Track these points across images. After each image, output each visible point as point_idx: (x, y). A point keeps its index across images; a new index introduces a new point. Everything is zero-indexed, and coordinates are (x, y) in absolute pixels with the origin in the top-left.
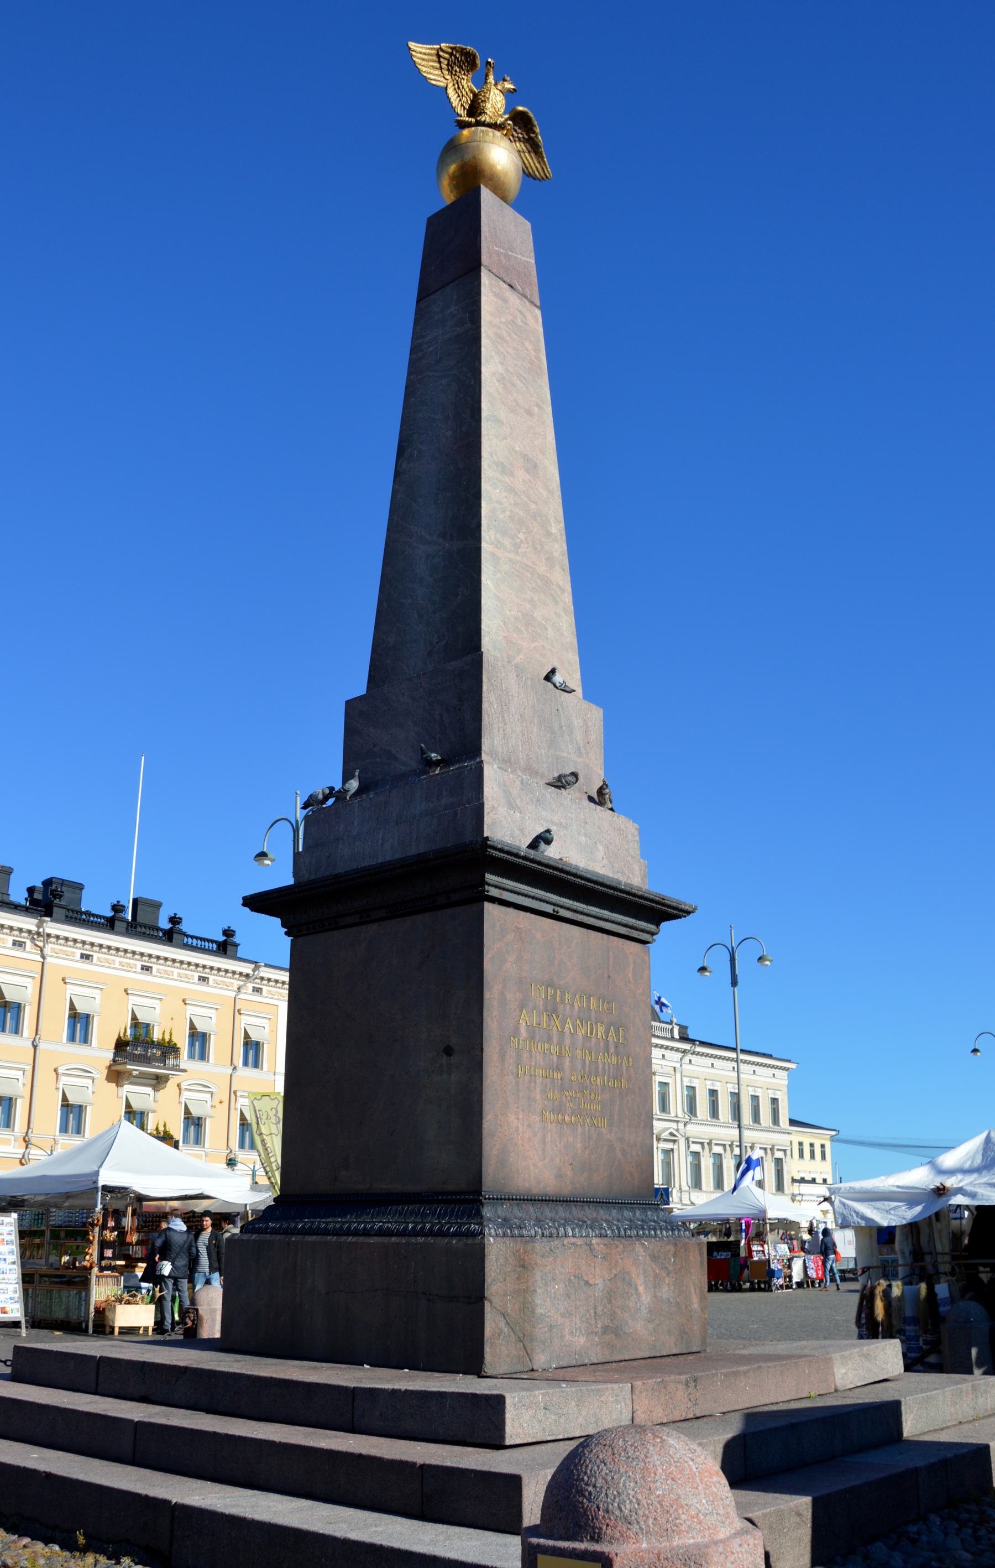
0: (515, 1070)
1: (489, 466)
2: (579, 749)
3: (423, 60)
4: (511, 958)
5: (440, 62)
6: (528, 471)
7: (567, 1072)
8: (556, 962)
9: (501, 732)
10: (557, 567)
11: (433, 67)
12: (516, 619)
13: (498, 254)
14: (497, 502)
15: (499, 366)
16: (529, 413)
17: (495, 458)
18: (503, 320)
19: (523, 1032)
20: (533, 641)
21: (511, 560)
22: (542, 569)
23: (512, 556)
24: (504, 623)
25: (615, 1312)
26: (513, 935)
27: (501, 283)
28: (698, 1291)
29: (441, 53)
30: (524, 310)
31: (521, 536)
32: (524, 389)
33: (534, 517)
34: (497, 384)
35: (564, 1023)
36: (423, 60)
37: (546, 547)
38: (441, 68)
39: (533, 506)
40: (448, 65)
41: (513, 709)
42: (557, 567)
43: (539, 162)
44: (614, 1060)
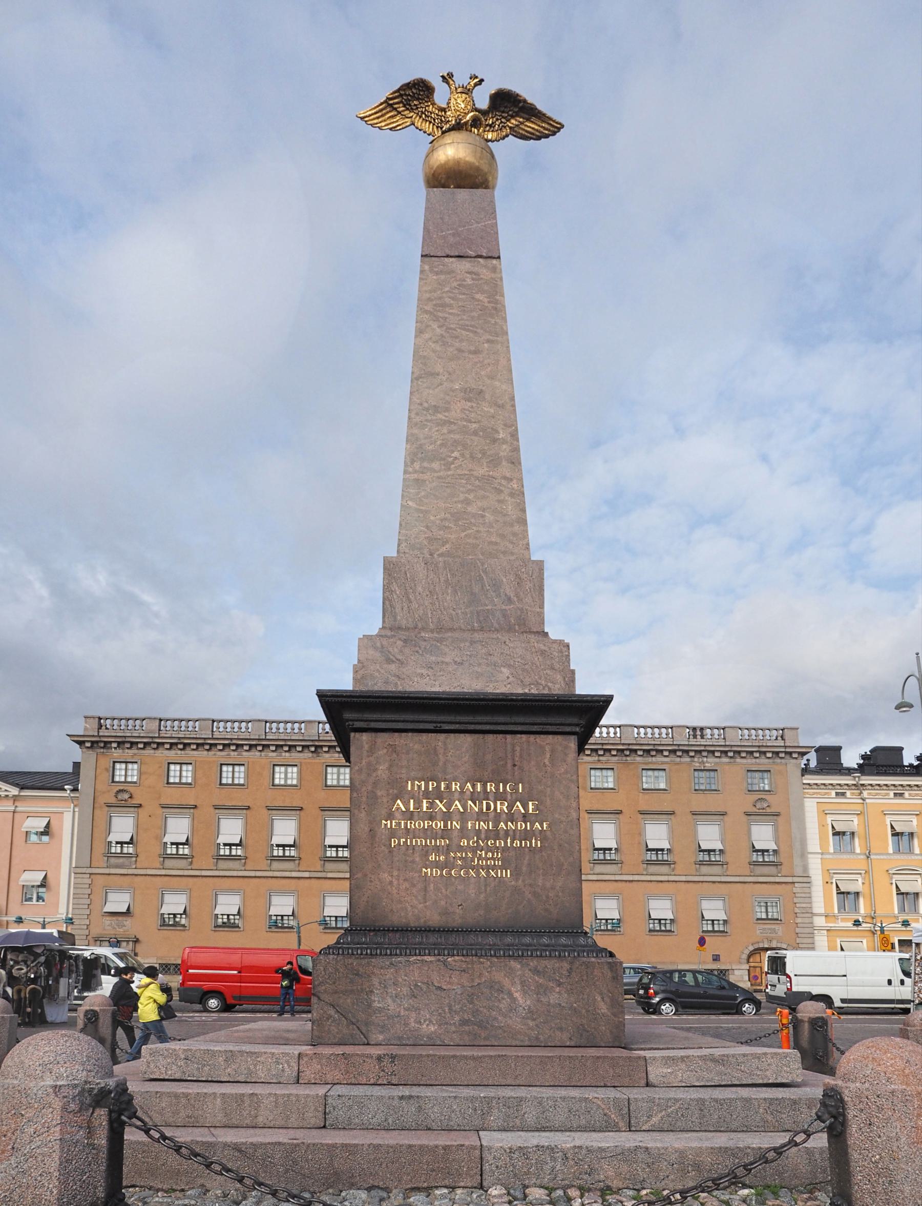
0: (388, 843)
1: (417, 414)
2: (509, 599)
3: (378, 118)
4: (382, 767)
5: (395, 109)
6: (469, 400)
7: (455, 841)
8: (441, 764)
9: (405, 609)
10: (504, 463)
11: (392, 117)
12: (441, 520)
13: (444, 237)
14: (425, 438)
15: (438, 330)
16: (476, 352)
17: (426, 405)
18: (447, 289)
19: (397, 815)
20: (463, 531)
21: (439, 478)
22: (482, 471)
23: (441, 474)
24: (427, 527)
25: (477, 1010)
26: (385, 751)
27: (446, 259)
28: (607, 1000)
29: (391, 102)
30: (476, 269)
31: (456, 454)
32: (471, 335)
33: (475, 433)
34: (433, 345)
35: (448, 806)
36: (378, 118)
37: (488, 453)
38: (399, 113)
39: (474, 425)
40: (404, 106)
41: (420, 589)
42: (504, 463)
43: (543, 121)
44: (521, 826)
